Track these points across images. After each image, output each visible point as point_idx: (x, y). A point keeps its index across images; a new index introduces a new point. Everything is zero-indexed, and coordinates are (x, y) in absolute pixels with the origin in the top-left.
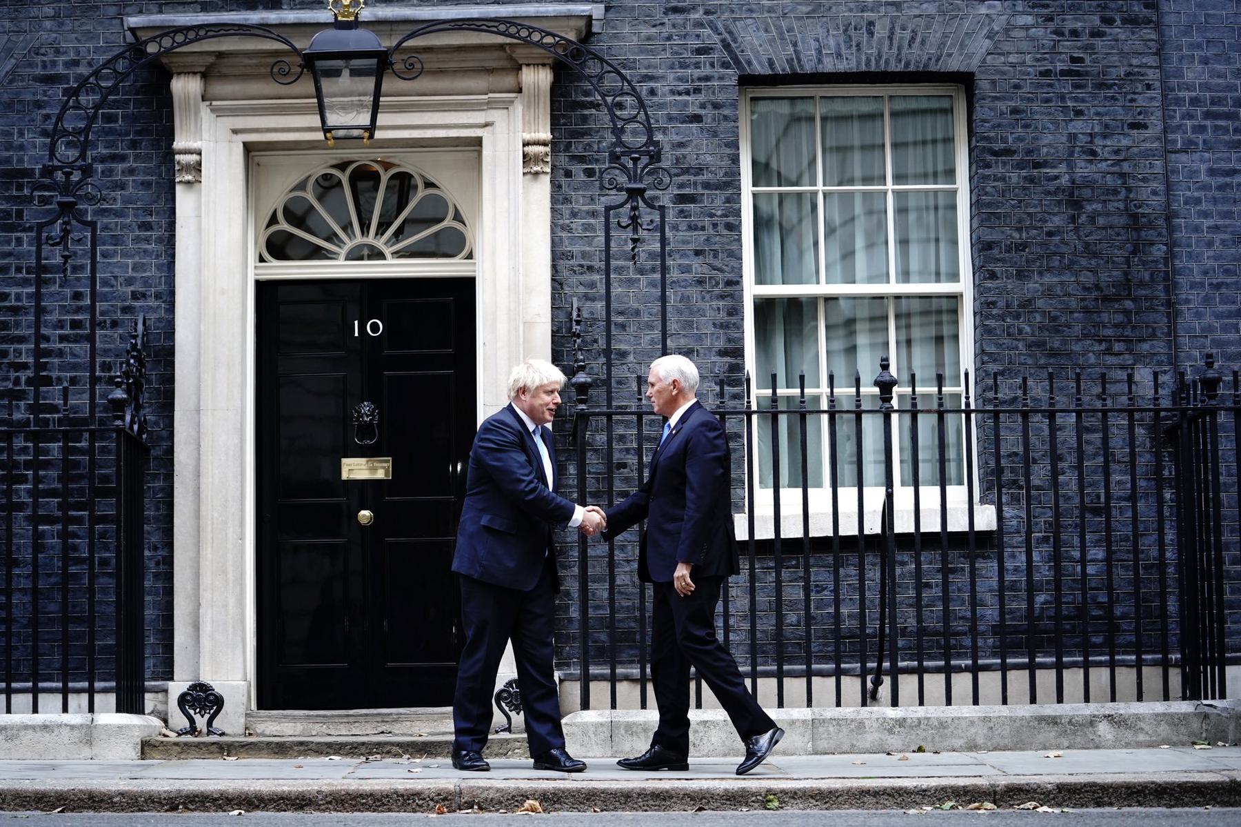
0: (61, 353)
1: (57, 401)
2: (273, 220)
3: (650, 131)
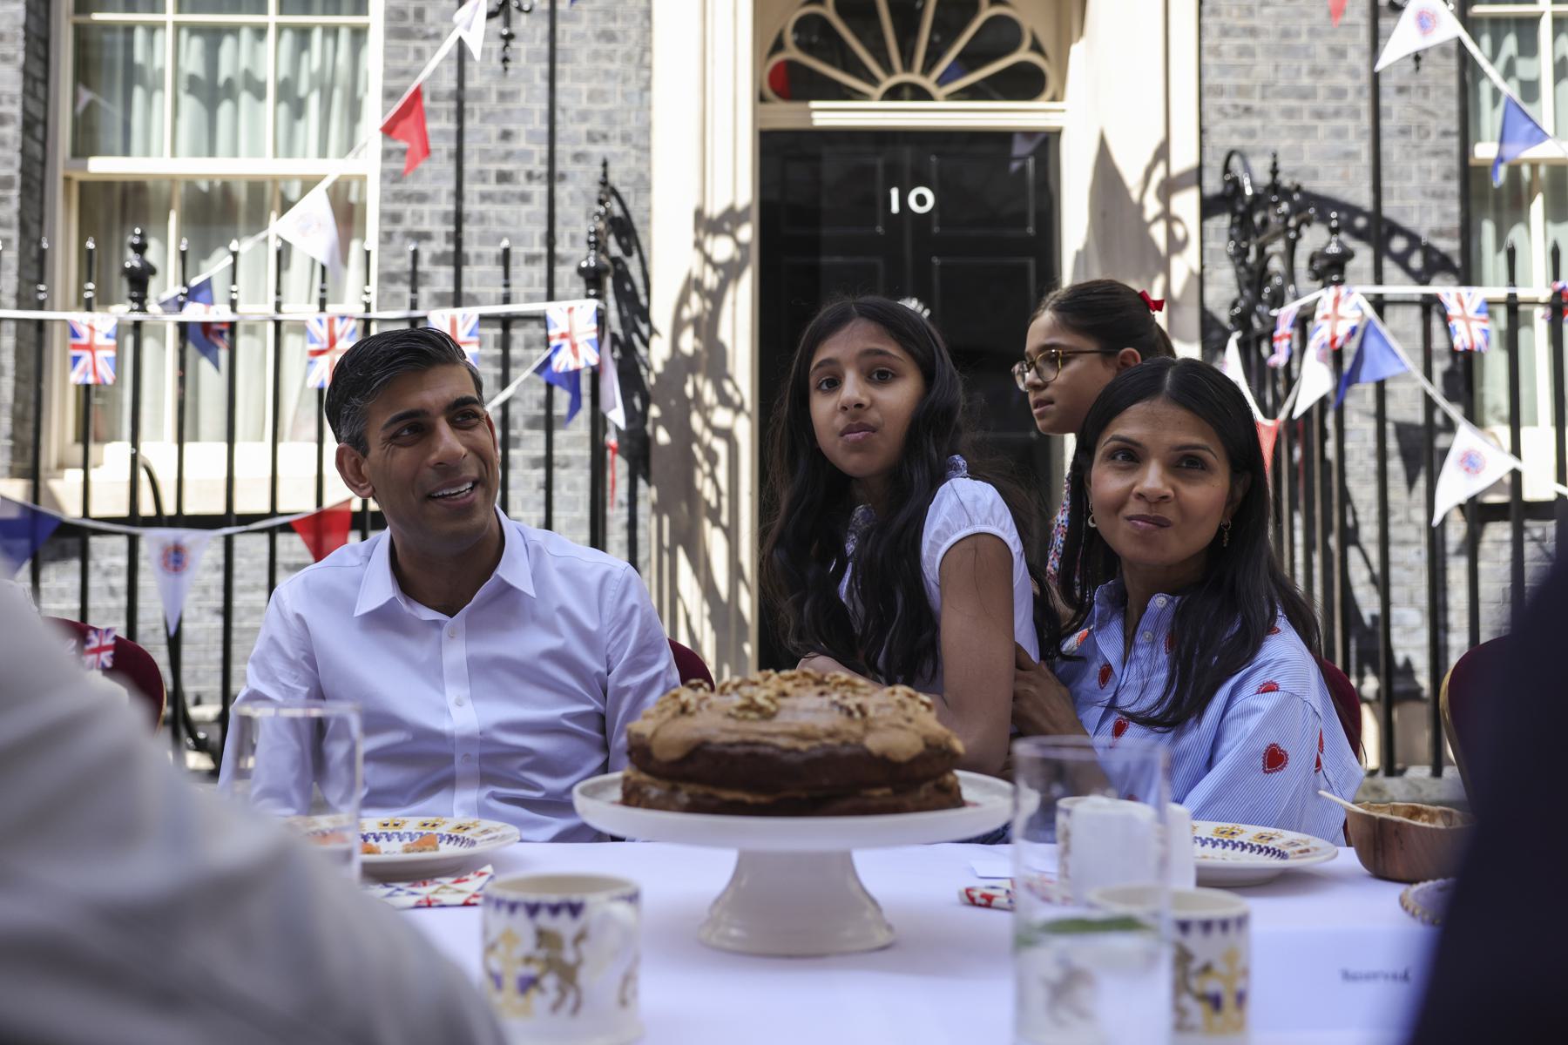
0: (482, 219)
2: (778, 46)
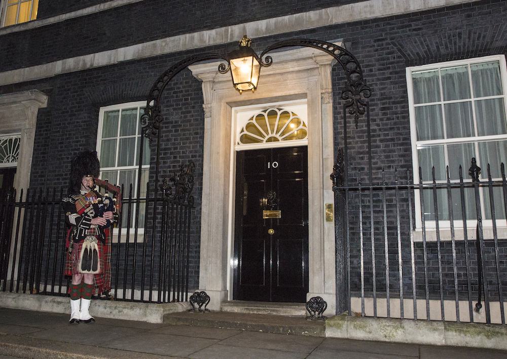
2: (242, 131)
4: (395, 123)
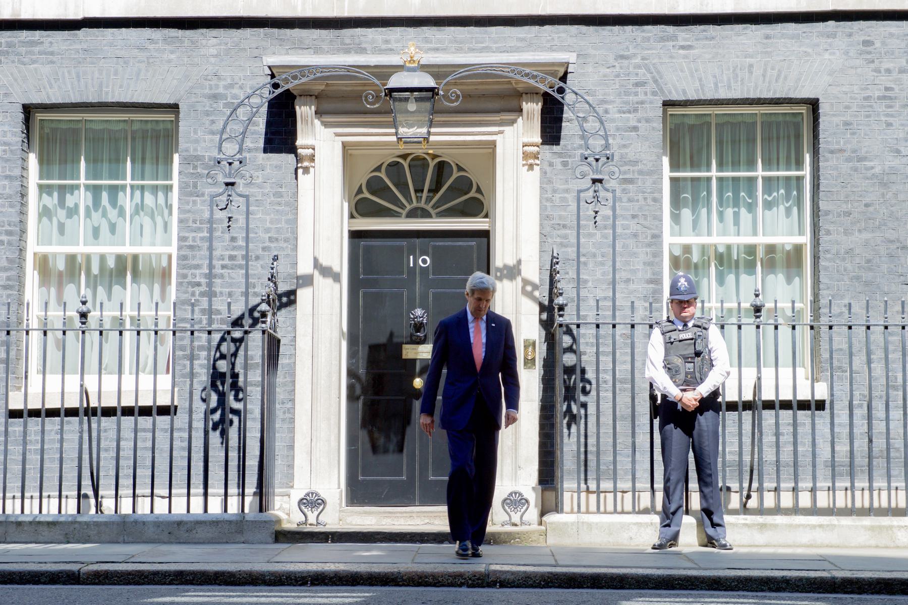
1: (219, 308)
2: (360, 191)
3: (606, 138)
4: (640, 208)
